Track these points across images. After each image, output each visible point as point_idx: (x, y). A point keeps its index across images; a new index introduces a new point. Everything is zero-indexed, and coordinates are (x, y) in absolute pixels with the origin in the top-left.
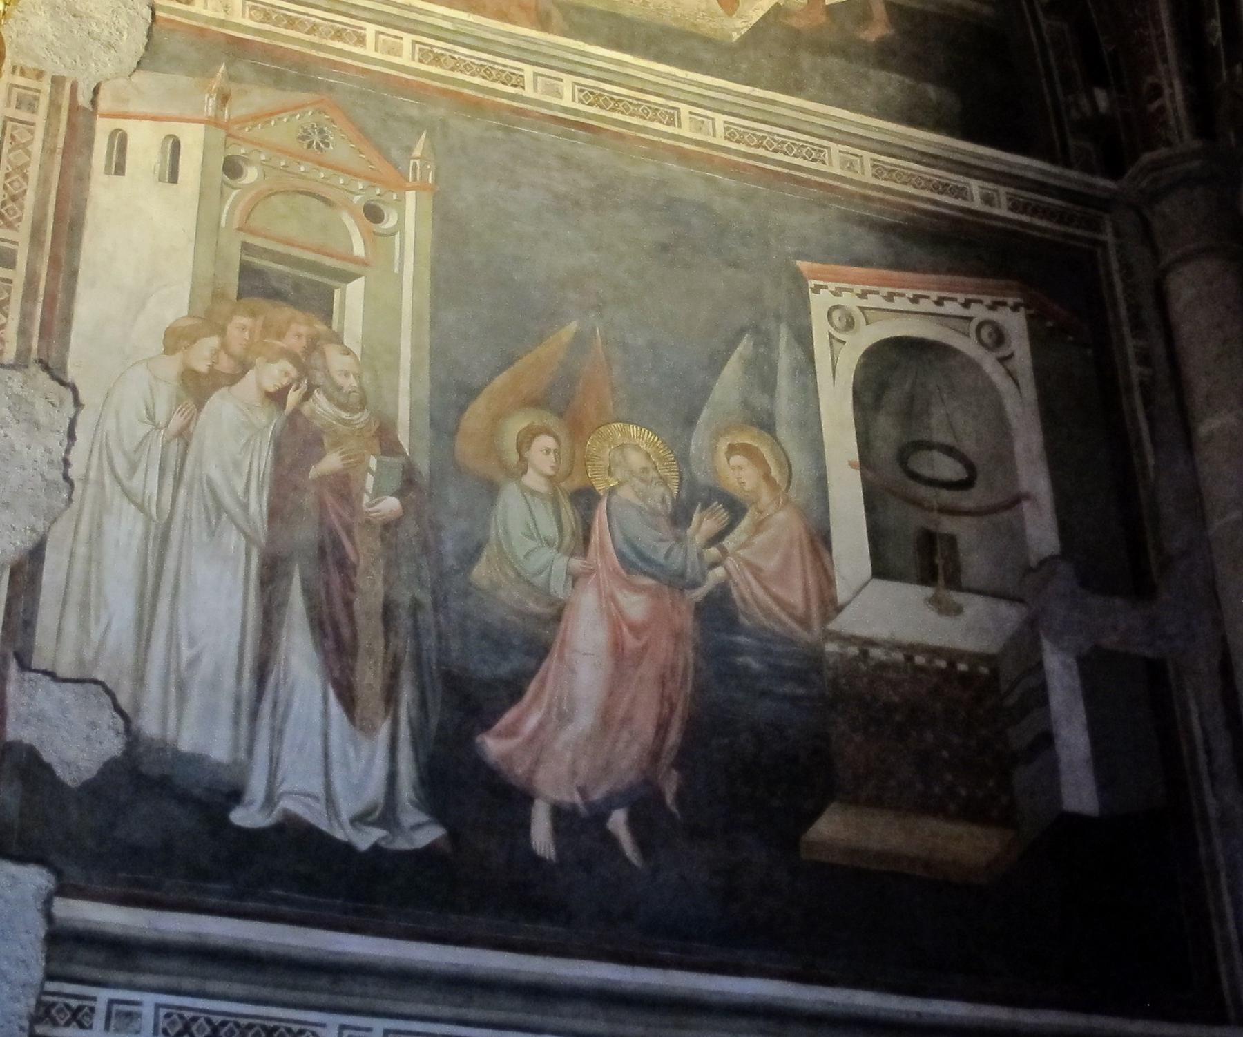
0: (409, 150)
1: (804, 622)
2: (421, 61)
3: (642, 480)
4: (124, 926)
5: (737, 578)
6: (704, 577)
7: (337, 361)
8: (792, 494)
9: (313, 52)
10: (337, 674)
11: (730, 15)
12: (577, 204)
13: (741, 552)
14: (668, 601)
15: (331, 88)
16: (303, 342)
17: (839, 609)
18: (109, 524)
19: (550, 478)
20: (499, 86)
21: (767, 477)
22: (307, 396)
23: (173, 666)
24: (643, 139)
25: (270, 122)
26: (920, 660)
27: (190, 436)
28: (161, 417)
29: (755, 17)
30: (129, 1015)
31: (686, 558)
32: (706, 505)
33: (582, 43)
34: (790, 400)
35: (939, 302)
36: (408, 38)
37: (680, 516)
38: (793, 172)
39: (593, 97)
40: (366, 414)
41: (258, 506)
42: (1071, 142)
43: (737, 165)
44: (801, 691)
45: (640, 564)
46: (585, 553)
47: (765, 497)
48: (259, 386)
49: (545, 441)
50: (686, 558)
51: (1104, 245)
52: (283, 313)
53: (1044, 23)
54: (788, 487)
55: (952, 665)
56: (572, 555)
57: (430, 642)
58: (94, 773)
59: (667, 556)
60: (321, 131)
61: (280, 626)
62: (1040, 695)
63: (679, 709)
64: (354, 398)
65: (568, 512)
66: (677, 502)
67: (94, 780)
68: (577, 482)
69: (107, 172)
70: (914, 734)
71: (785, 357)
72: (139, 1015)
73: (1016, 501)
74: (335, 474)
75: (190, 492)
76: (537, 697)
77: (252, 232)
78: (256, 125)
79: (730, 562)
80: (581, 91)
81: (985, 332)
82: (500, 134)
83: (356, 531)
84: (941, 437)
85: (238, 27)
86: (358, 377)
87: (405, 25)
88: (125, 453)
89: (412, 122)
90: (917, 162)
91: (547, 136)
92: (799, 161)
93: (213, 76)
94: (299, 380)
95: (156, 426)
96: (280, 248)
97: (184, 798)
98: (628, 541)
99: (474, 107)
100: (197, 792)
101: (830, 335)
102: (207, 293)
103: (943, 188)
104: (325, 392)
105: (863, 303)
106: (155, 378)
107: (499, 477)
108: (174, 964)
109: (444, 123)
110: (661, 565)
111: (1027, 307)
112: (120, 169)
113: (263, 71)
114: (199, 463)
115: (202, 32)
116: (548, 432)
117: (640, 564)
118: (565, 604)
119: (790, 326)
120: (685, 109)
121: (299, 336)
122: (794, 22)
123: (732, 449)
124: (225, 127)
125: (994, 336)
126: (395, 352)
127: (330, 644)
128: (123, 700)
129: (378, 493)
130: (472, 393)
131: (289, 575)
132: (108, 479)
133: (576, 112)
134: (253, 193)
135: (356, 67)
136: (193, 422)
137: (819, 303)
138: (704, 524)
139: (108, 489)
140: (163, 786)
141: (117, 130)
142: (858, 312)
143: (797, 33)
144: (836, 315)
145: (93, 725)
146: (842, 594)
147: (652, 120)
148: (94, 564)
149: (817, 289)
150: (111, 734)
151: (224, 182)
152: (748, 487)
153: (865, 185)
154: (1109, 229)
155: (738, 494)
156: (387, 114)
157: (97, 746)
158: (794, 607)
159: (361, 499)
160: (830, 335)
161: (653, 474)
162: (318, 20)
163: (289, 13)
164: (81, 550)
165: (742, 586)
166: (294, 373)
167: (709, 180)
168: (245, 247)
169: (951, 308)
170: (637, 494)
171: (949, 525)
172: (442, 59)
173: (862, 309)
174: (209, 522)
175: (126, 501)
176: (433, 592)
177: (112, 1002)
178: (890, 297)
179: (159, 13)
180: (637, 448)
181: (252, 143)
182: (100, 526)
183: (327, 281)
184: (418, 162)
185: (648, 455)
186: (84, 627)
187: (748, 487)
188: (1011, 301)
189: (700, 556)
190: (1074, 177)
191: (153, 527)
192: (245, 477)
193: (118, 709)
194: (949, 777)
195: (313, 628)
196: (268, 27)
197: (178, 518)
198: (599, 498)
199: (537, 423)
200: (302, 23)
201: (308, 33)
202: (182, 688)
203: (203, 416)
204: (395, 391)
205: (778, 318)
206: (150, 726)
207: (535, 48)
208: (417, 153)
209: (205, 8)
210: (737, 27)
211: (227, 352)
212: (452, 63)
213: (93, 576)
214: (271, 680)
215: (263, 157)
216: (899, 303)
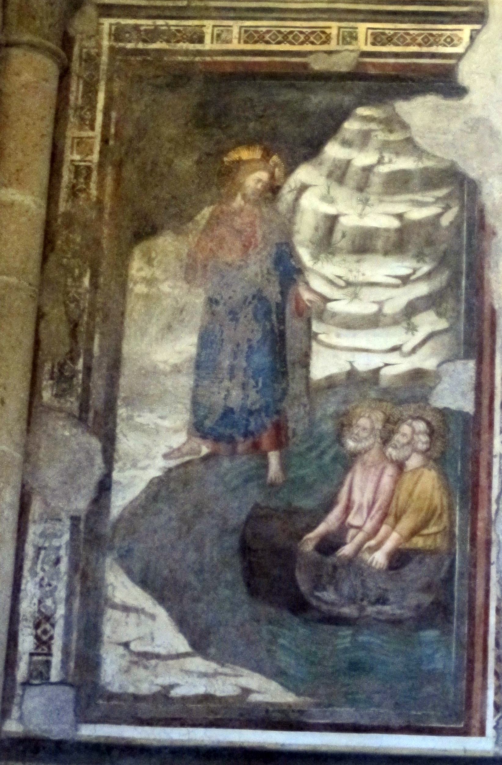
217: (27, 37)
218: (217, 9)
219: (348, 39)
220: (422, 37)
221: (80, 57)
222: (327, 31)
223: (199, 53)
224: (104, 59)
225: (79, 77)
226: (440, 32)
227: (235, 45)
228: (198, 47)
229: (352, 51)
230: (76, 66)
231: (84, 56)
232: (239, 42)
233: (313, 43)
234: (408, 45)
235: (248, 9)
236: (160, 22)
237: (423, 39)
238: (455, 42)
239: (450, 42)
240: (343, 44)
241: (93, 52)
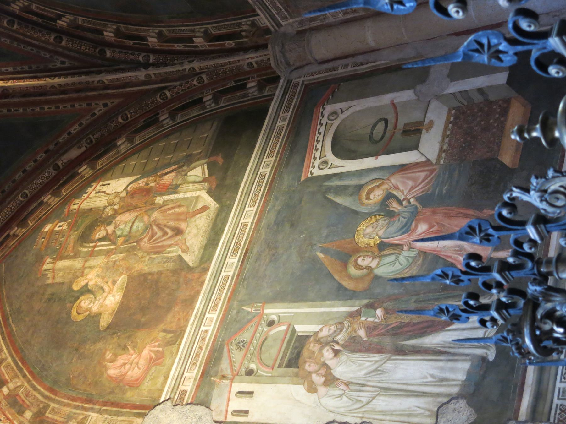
0: (248, 313)
1: (432, 171)
2: (216, 311)
3: (376, 228)
4: (530, 396)
5: (414, 194)
6: (413, 205)
7: (325, 333)
8: (385, 178)
9: (209, 348)
10: (440, 327)
11: (209, 208)
12: (273, 255)
13: (405, 194)
14: (421, 217)
15: (223, 340)
16: (317, 345)
17: (428, 160)
18: (379, 409)
19: (373, 259)
20: (228, 284)
21: (378, 186)
22: (337, 343)
23: (433, 384)
24: (252, 234)
25: (234, 361)
26: (448, 133)
27: (348, 382)
28: (340, 392)
29: (210, 199)
30: (563, 392)
31: (405, 212)
32: (388, 206)
33: (215, 257)
34: (351, 180)
35: (320, 133)
36: (207, 315)
37: (391, 215)
38: (268, 184)
39: (235, 251)
40: (345, 322)
41: (376, 357)
42: (266, 94)
43: (264, 202)
44: (457, 172)
45: (407, 226)
46: (402, 245)
47: (386, 186)
48: (331, 359)
49: (360, 261)
50: (405, 212)
51: (303, 81)
52: (305, 353)
53: (222, 105)
54: (384, 179)
55: (451, 122)
56: (402, 250)
57: (431, 296)
58: (471, 409)
59: (405, 218)
60: (239, 343)
61: (422, 347)
62: (464, 93)
63: (462, 211)
64: (339, 326)
65: (386, 252)
66: (385, 216)
67: (474, 409)
68: (376, 250)
69: (247, 416)
70: (475, 133)
71: (336, 183)
72: (564, 388)
73: (393, 104)
74: (366, 331)
75: (370, 381)
76: (454, 259)
77: (274, 365)
78: (235, 366)
79: (408, 197)
80: (232, 256)
81: (332, 118)
82: (246, 282)
83: (387, 323)
84: (369, 130)
85: (197, 374)
86: (331, 325)
87: (202, 317)
88: (353, 404)
89: (238, 312)
90: (269, 144)
91: (248, 267)
92: (265, 182)
93: (215, 381)
94: (330, 345)
95: (344, 394)
96: (281, 355)
97: (484, 377)
98: (397, 232)
99: (234, 292)
100: (481, 373)
101: (329, 168)
102: (295, 379)
103: (279, 134)
104: (336, 336)
105: (318, 158)
106: (326, 395)
107: (372, 275)
108: (545, 376)
109: (239, 301)
110: (408, 219)
111: (324, 105)
112: (247, 412)
113: (214, 365)
114: (358, 378)
115: (198, 386)
116: (356, 261)
117: (407, 226)
118: (420, 251)
119: (325, 182)
120: (242, 221)
121: (314, 346)
122: (214, 187)
123: (368, 198)
124: (234, 376)
125: (334, 115)
126: (322, 313)
127: (429, 330)
128: (445, 400)
129: (375, 316)
130: (340, 287)
131: (403, 345)
132: (363, 410)
133: (240, 257)
134: (260, 365)
135: (216, 332)
136: (344, 381)
137: (316, 172)
138: (395, 206)
139: (366, 409)
140: (478, 386)
141: (232, 414)
142: (321, 160)
143: (218, 186)
144: (321, 167)
145: (454, 410)
146: (423, 159)
147: (245, 232)
148: (394, 413)
149: (312, 174)
150: (458, 404)
151: (255, 375)
152: (381, 192)
153: (275, 160)
154: (298, 80)
155: (384, 195)
156: (234, 321)
157: (462, 409)
158: (427, 175)
159: (376, 322)
160: (329, 168)
161: (375, 224)
162: (198, 347)
163: (194, 357)
164: (388, 418)
165: (418, 192)
166: (327, 348)
167: (268, 212)
168: (279, 366)
169: (322, 129)
170: (381, 229)
171: (400, 126)
172: (216, 303)
173: (320, 158)
174: (381, 374)
175: (371, 403)
176: (412, 295)
177: (559, 398)
178: (316, 150)
179: (189, 402)
180: (365, 230)
181: (241, 367)
182: (380, 412)
183: (294, 338)
184: (253, 309)
185: (367, 226)
186: (416, 416)
187: (381, 192)
188: (321, 110)
189: (405, 207)
190: (278, 93)
191: (381, 393)
192: (365, 362)
193: (447, 403)
194: (491, 121)
195: (424, 336)
196: (198, 364)
197: (379, 385)
198: (382, 241)
199: (353, 264)
200: (198, 352)
201: (202, 350)
202: (442, 380)
203: (341, 378)
204: (337, 312)
205: (321, 186)
206: (455, 390)
207: (215, 272)
208: (250, 310)
209: (189, 386)
210: (213, 205)
211: (318, 371)
212: (218, 300)
213: (398, 413)
214: (441, 349)
215: (247, 362)
216: (319, 146)
217: (309, 57)
221: (302, 27)
224: (297, 19)
225: (310, 25)
230: (307, 27)
231: (301, 26)
241: (297, 23)
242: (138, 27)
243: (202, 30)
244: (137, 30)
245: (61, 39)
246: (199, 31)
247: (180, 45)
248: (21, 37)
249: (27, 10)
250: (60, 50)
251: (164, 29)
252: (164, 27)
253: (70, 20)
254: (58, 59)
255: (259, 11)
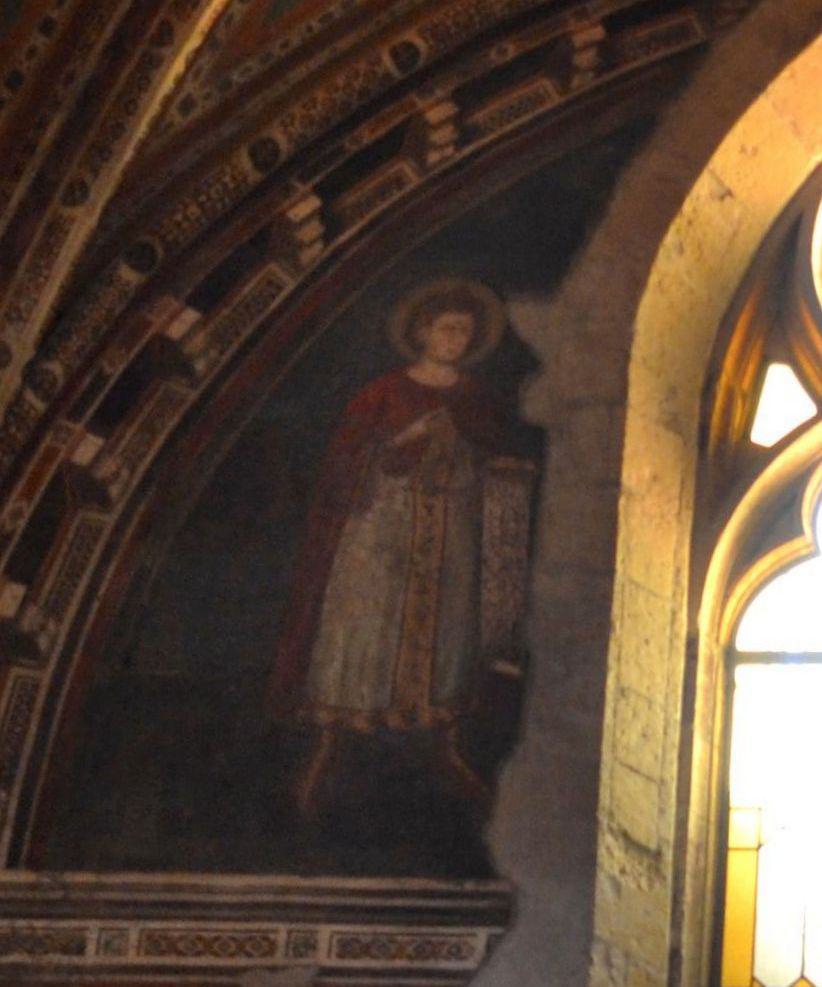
218: (109, 903)
219: (302, 950)
220: (414, 945)
222: (272, 936)
223: (78, 970)
226: (442, 939)
227: (132, 958)
228: (76, 960)
229: (307, 967)
232: (138, 954)
233: (249, 955)
234: (394, 957)
235: (155, 904)
236: (21, 923)
237: (415, 949)
238: (464, 954)
239: (457, 953)
240: (296, 956)
242: (161, 439)
243: (43, 643)
244: (150, 429)
245: (259, 165)
246: (43, 628)
247: (22, 523)
248: (343, 44)
249: (406, 139)
250: (228, 129)
251: (110, 519)
252: (119, 529)
253: (301, 246)
254: (207, 97)
255: (24, 877)
